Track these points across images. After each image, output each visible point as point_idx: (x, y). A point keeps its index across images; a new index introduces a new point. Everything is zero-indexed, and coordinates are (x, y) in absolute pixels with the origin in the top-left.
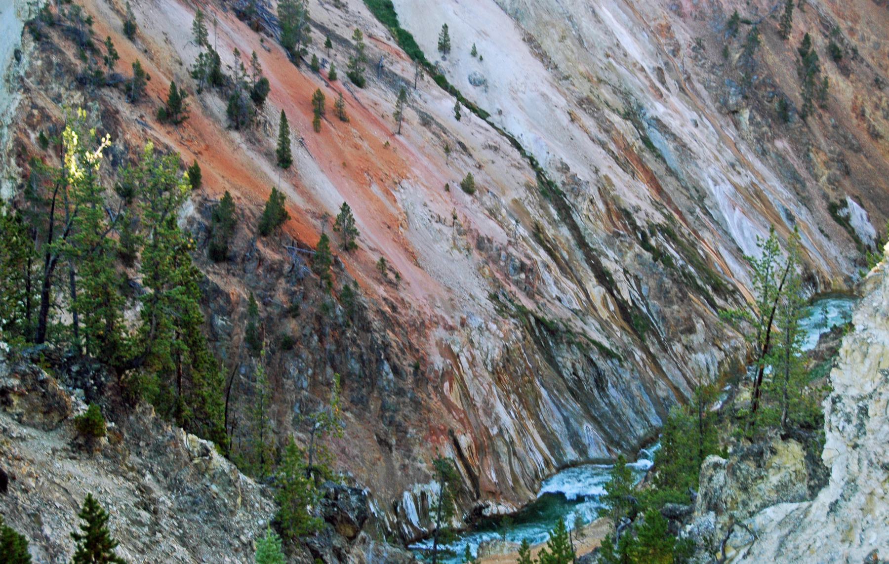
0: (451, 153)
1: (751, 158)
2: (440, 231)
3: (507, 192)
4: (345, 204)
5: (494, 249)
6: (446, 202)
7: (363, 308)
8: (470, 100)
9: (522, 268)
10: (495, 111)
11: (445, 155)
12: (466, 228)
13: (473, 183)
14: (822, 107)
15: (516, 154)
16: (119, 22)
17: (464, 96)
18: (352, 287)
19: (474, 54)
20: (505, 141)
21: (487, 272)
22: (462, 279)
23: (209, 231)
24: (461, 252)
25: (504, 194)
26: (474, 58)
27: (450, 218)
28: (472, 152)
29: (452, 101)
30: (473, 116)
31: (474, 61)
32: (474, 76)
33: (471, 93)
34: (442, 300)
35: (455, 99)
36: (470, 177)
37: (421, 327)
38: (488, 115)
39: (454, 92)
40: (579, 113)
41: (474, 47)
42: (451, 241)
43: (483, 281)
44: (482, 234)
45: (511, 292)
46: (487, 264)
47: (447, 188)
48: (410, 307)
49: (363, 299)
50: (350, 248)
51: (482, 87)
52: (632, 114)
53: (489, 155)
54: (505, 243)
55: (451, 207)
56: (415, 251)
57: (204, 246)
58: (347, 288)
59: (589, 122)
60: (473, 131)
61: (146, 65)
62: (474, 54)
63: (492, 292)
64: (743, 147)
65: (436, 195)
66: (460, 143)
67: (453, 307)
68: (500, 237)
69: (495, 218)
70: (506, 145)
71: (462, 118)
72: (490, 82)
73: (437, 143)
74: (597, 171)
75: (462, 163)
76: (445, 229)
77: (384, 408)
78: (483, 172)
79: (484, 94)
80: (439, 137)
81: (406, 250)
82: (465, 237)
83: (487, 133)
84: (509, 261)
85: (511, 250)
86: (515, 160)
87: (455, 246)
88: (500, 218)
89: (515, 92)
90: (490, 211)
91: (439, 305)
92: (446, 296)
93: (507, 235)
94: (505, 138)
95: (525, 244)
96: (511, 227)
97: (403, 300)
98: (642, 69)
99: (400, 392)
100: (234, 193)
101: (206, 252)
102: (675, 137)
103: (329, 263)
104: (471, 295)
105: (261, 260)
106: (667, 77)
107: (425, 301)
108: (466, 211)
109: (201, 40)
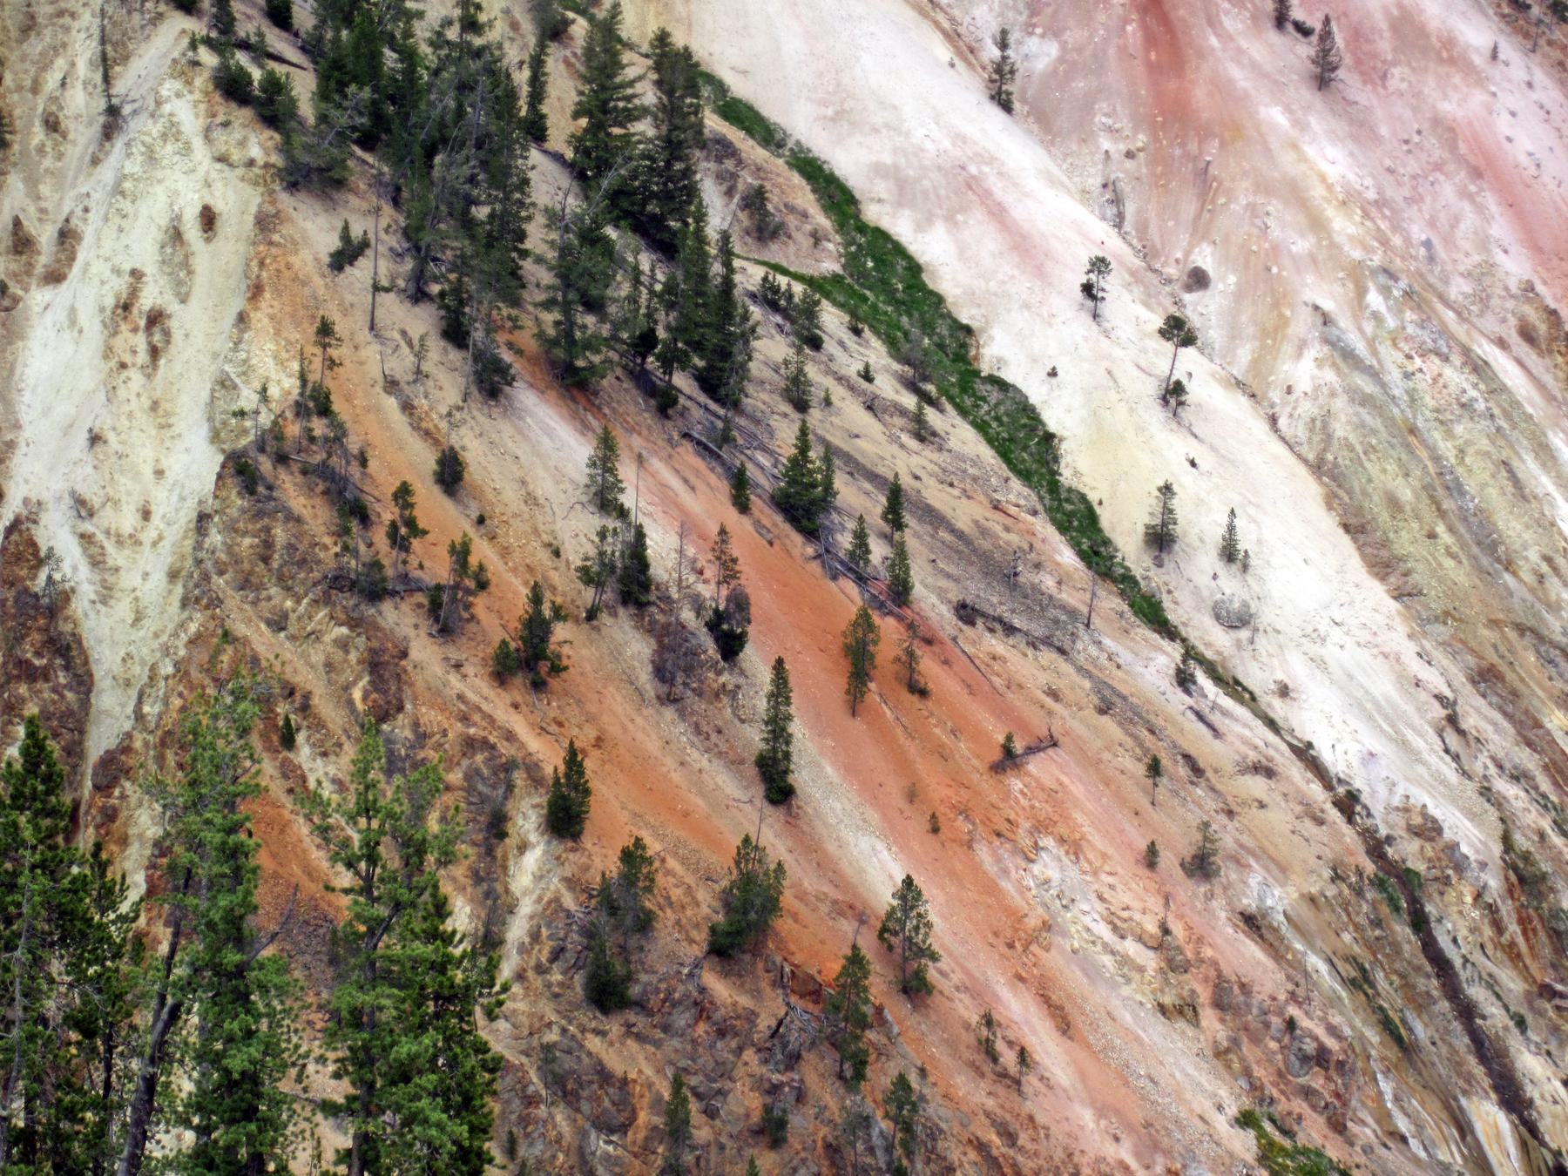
4: (908, 882)
5: (1255, 1011)
7: (934, 1133)
9: (1321, 1058)
15: (1316, 790)
16: (426, 459)
18: (913, 1079)
23: (590, 933)
33: (1215, 639)
49: (935, 1110)
50: (915, 988)
57: (576, 967)
58: (902, 1082)
61: (482, 551)
66: (1187, 757)
97: (1031, 1118)
100: (653, 846)
101: (579, 979)
103: (864, 1024)
105: (702, 1007)
109: (605, 500)
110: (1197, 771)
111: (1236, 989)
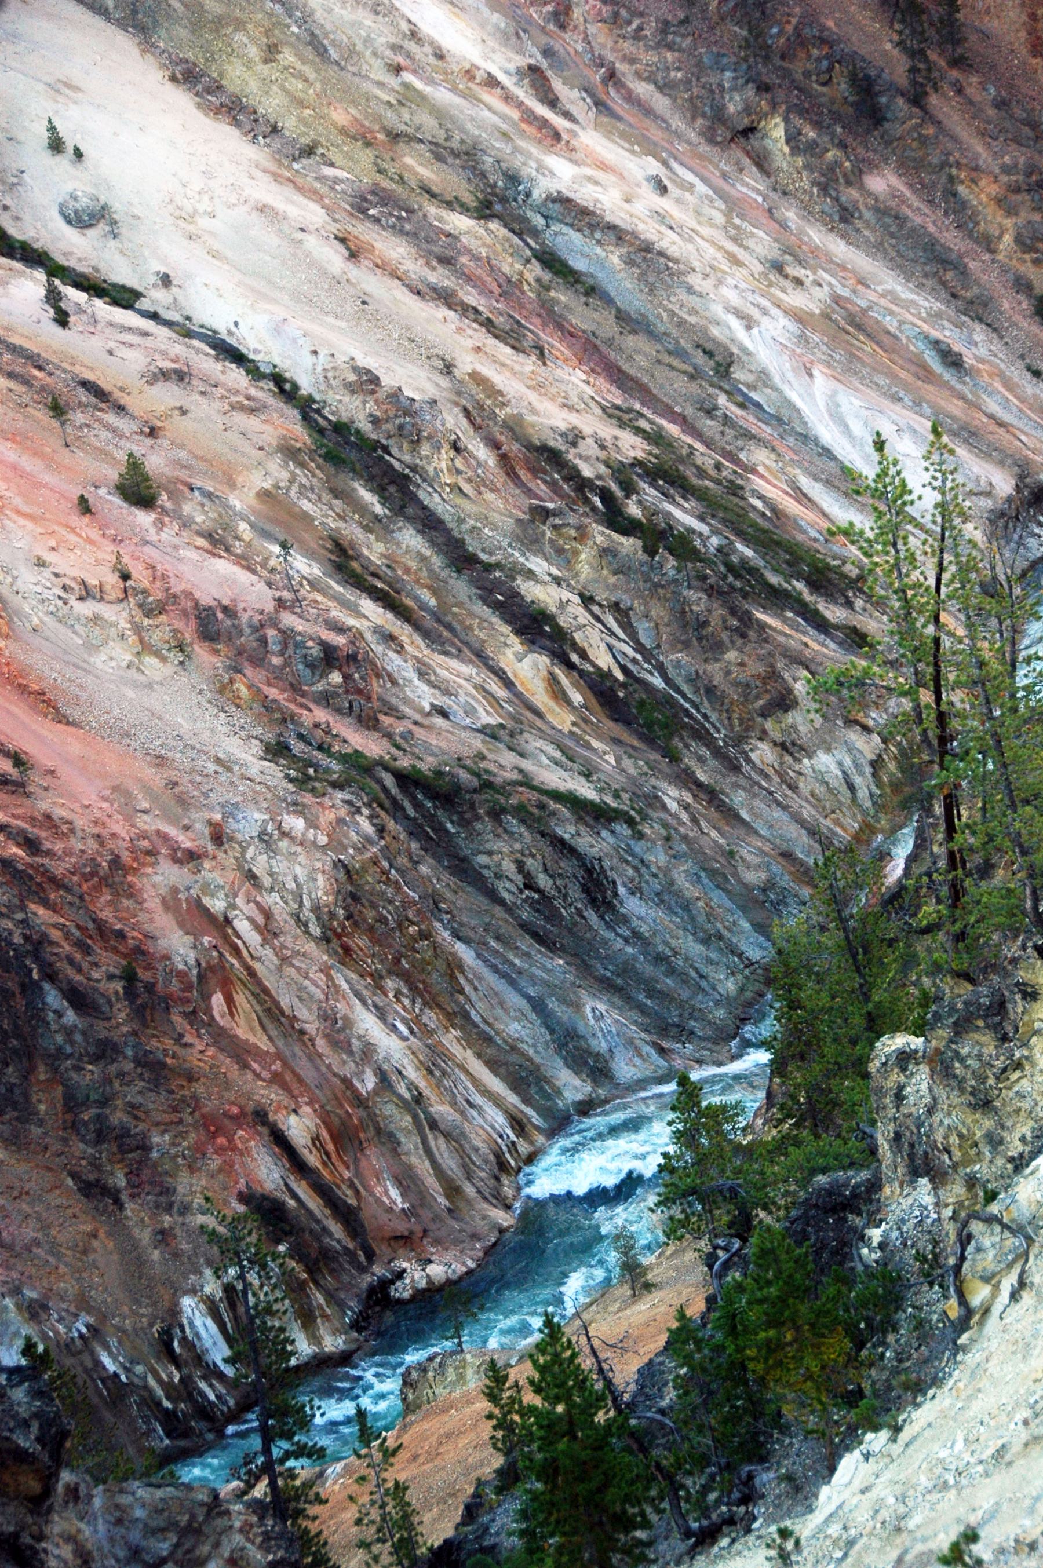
0: (71, 415)
1: (816, 235)
2: (96, 619)
3: (240, 480)
5: (247, 631)
6: (90, 541)
8: (82, 268)
9: (330, 658)
10: (153, 279)
11: (55, 423)
12: (160, 595)
13: (147, 479)
14: (956, 62)
15: (236, 376)
17: (62, 261)
19: (56, 145)
20: (198, 351)
21: (244, 692)
22: (184, 724)
24: (164, 659)
25: (232, 485)
26: (59, 158)
27: (112, 580)
28: (124, 400)
29: (36, 281)
30: (100, 306)
31: (63, 163)
32: (72, 204)
34: (147, 790)
35: (40, 275)
36: (134, 465)
37: (114, 874)
38: (137, 295)
39: (32, 256)
40: (364, 232)
41: (52, 129)
42: (133, 639)
43: (241, 718)
44: (206, 600)
45: (317, 725)
46: (239, 672)
47: (84, 506)
48: (72, 831)
51: (102, 227)
52: (497, 199)
53: (164, 397)
54: (270, 607)
55: (107, 552)
56: (45, 685)
59: (395, 250)
60: (112, 344)
62: (56, 145)
63: (270, 737)
64: (791, 215)
65: (63, 531)
66: (85, 384)
67: (183, 801)
68: (253, 594)
69: (227, 550)
70: (205, 362)
71: (72, 319)
72: (118, 209)
73: (26, 399)
74: (448, 369)
75: (105, 434)
76: (108, 612)
77: (72, 1103)
78: (166, 443)
79: (112, 243)
80: (25, 381)
81: (23, 689)
82: (163, 618)
83: (149, 342)
84: (290, 651)
85: (288, 620)
86: (237, 392)
87: (146, 648)
88: (238, 548)
89: (190, 218)
90: (209, 536)
91: (145, 805)
92: (156, 778)
93: (269, 584)
94: (196, 343)
95: (320, 598)
96: (272, 563)
97: (48, 817)
98: (492, 82)
99: (105, 1051)
102: (617, 234)
104: (218, 761)
106: (558, 86)
107: (105, 805)
108: (147, 549)
110: (100, 394)
111: (220, 616)
